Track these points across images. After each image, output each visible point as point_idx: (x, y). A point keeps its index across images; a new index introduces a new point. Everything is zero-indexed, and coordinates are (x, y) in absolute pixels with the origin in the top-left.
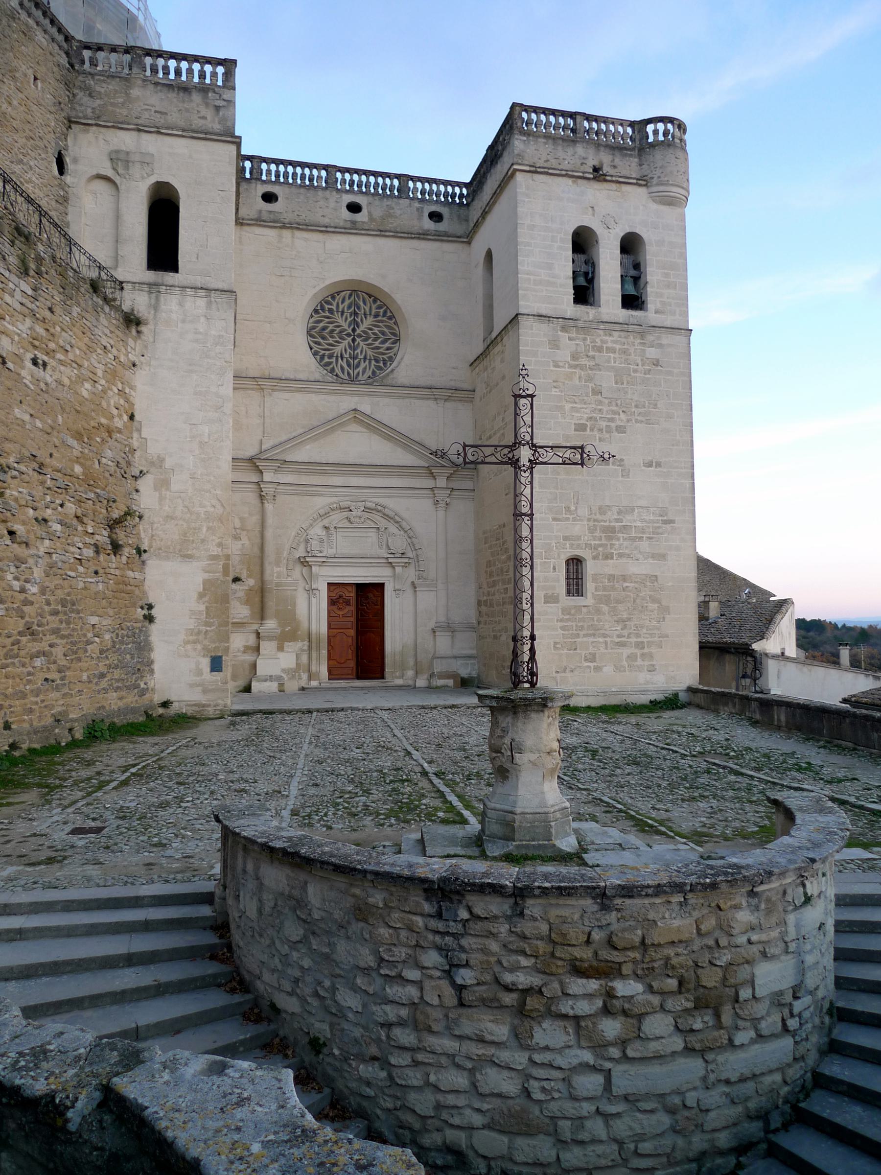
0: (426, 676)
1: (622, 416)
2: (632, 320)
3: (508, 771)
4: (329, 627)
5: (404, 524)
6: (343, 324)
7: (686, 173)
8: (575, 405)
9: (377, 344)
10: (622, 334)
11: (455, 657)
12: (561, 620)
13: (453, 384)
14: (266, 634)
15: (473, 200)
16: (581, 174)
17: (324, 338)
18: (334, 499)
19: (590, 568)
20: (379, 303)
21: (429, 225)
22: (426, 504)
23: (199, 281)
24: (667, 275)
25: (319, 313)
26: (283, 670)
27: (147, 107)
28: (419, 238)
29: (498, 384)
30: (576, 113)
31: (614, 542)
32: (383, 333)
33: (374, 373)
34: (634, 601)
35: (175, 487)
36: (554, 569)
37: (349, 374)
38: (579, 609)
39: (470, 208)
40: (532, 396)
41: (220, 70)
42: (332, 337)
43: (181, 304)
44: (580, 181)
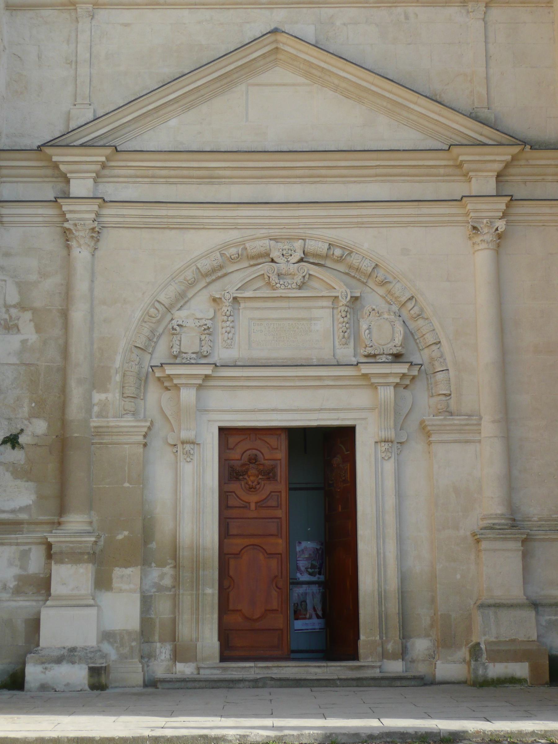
18: (233, 235)
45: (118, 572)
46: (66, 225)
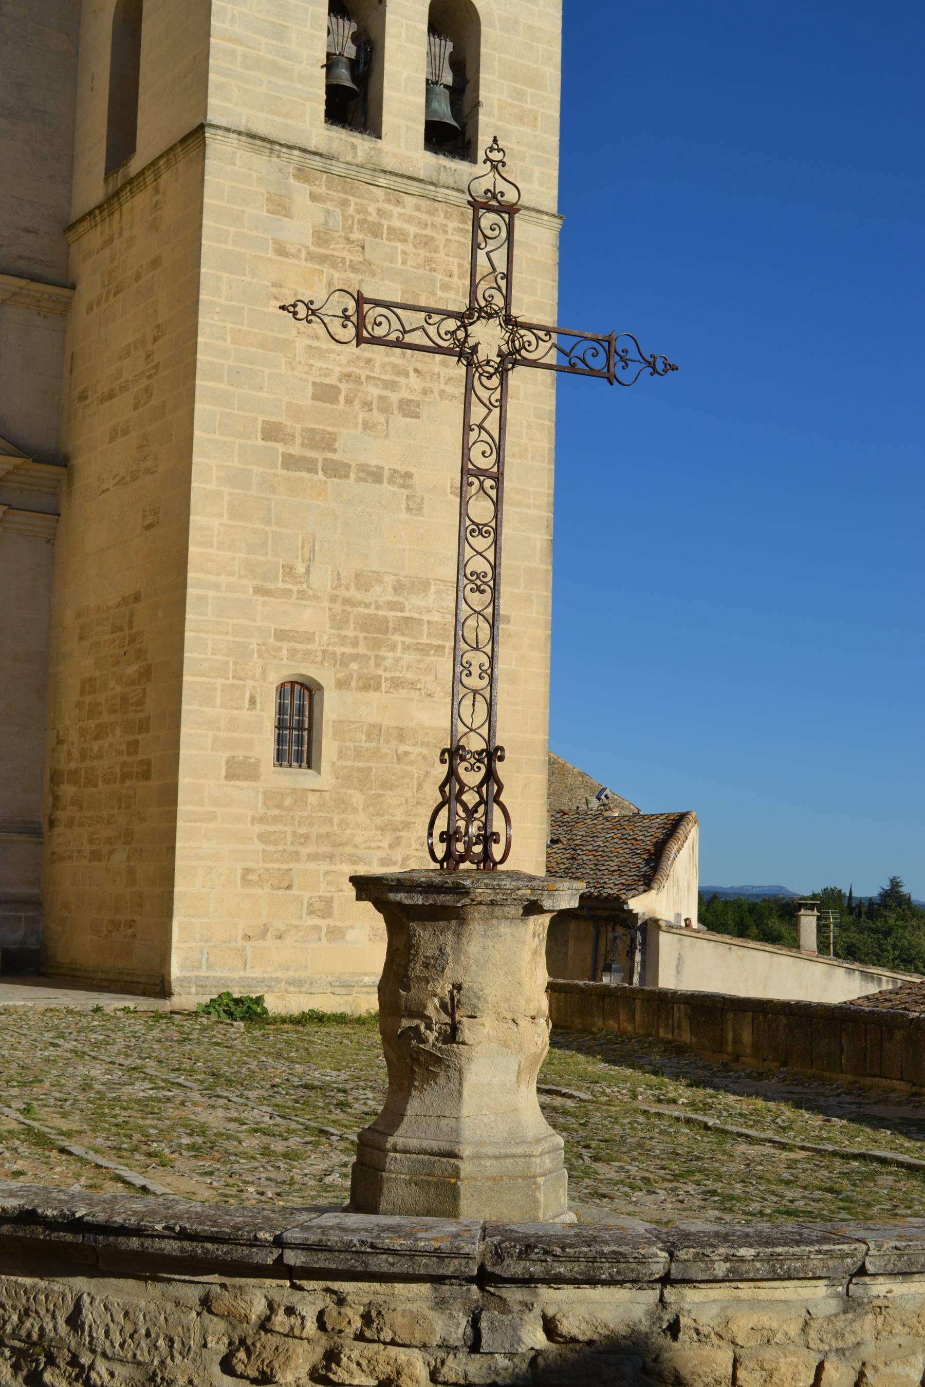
1: (414, 380)
2: (443, 178)
8: (316, 343)
10: (424, 203)
12: (262, 820)
19: (333, 708)
24: (519, 95)
29: (138, 277)
31: (382, 653)
34: (420, 786)
36: (253, 702)
38: (300, 796)
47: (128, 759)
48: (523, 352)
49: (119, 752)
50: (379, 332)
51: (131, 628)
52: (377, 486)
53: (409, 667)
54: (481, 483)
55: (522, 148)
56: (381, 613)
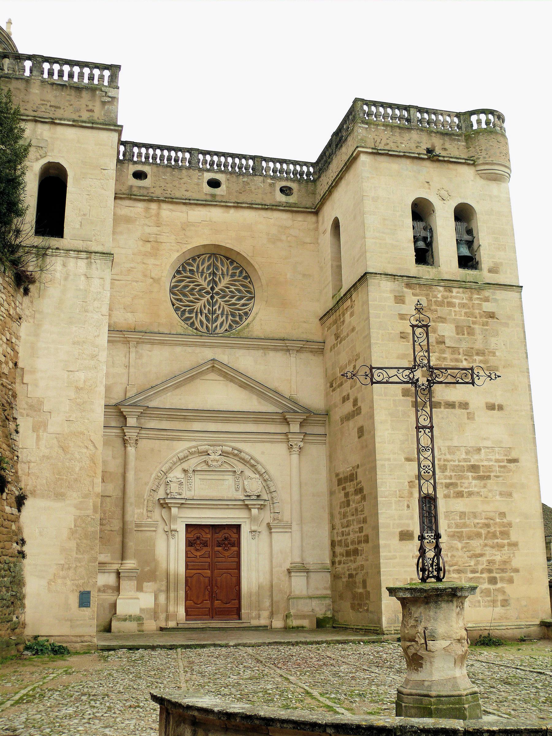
0: (281, 616)
3: (422, 658)
4: (187, 568)
5: (259, 467)
6: (202, 283)
7: (507, 154)
9: (233, 301)
10: (461, 290)
11: (310, 598)
13: (304, 336)
14: (126, 574)
15: (319, 177)
16: (417, 155)
17: (185, 295)
18: (194, 443)
20: (235, 264)
21: (281, 198)
22: (282, 448)
23: (80, 245)
25: (181, 274)
26: (142, 610)
27: (43, 102)
28: (272, 209)
30: (410, 107)
32: (239, 291)
33: (230, 326)
35: (51, 429)
37: (207, 327)
39: (318, 183)
40: (427, 326)
41: (107, 73)
42: (193, 295)
43: (64, 265)
44: (415, 161)
45: (145, 584)
46: (125, 437)
47: (360, 535)
48: (437, 379)
49: (356, 532)
50: (379, 379)
51: (356, 479)
52: (453, 410)
53: (475, 486)
54: (425, 431)
55: (501, 261)
56: (461, 464)
